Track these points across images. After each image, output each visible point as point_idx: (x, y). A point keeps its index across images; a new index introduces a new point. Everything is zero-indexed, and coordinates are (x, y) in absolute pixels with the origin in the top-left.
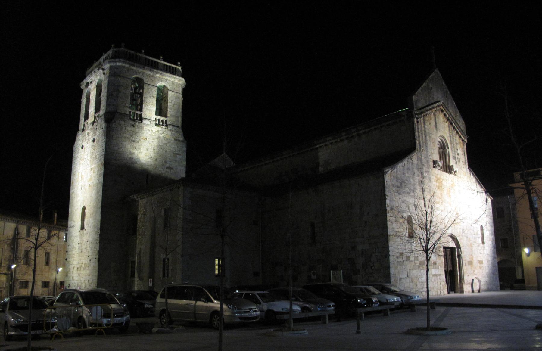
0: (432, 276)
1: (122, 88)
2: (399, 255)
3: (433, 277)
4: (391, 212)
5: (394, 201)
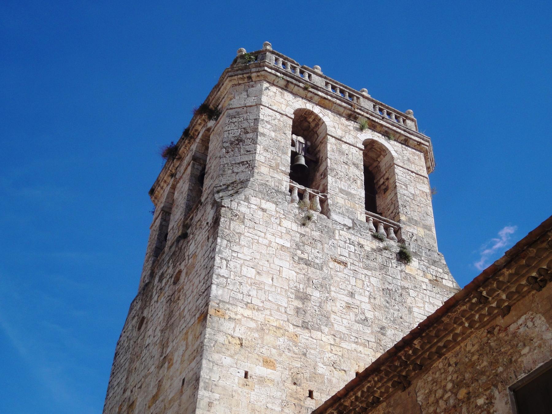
1: (269, 126)
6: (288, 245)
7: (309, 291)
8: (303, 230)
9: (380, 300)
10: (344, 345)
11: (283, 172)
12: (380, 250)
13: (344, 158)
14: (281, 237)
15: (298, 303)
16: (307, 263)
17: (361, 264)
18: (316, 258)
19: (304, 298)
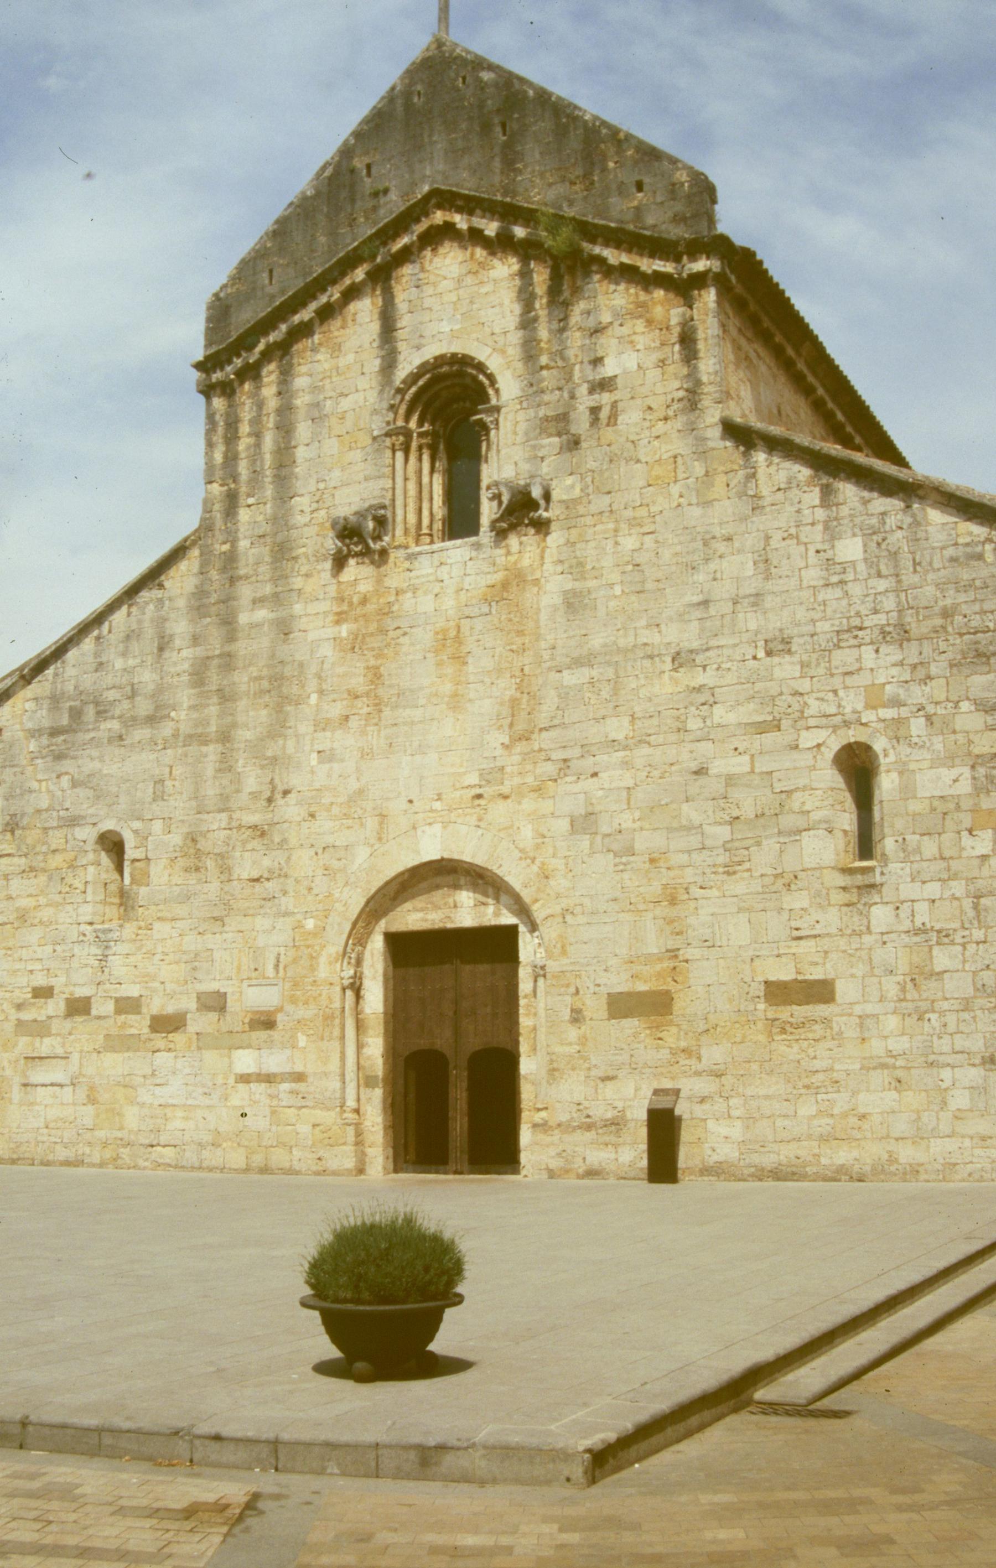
0: (231, 1081)
2: (30, 995)
4: (8, 835)
5: (30, 791)
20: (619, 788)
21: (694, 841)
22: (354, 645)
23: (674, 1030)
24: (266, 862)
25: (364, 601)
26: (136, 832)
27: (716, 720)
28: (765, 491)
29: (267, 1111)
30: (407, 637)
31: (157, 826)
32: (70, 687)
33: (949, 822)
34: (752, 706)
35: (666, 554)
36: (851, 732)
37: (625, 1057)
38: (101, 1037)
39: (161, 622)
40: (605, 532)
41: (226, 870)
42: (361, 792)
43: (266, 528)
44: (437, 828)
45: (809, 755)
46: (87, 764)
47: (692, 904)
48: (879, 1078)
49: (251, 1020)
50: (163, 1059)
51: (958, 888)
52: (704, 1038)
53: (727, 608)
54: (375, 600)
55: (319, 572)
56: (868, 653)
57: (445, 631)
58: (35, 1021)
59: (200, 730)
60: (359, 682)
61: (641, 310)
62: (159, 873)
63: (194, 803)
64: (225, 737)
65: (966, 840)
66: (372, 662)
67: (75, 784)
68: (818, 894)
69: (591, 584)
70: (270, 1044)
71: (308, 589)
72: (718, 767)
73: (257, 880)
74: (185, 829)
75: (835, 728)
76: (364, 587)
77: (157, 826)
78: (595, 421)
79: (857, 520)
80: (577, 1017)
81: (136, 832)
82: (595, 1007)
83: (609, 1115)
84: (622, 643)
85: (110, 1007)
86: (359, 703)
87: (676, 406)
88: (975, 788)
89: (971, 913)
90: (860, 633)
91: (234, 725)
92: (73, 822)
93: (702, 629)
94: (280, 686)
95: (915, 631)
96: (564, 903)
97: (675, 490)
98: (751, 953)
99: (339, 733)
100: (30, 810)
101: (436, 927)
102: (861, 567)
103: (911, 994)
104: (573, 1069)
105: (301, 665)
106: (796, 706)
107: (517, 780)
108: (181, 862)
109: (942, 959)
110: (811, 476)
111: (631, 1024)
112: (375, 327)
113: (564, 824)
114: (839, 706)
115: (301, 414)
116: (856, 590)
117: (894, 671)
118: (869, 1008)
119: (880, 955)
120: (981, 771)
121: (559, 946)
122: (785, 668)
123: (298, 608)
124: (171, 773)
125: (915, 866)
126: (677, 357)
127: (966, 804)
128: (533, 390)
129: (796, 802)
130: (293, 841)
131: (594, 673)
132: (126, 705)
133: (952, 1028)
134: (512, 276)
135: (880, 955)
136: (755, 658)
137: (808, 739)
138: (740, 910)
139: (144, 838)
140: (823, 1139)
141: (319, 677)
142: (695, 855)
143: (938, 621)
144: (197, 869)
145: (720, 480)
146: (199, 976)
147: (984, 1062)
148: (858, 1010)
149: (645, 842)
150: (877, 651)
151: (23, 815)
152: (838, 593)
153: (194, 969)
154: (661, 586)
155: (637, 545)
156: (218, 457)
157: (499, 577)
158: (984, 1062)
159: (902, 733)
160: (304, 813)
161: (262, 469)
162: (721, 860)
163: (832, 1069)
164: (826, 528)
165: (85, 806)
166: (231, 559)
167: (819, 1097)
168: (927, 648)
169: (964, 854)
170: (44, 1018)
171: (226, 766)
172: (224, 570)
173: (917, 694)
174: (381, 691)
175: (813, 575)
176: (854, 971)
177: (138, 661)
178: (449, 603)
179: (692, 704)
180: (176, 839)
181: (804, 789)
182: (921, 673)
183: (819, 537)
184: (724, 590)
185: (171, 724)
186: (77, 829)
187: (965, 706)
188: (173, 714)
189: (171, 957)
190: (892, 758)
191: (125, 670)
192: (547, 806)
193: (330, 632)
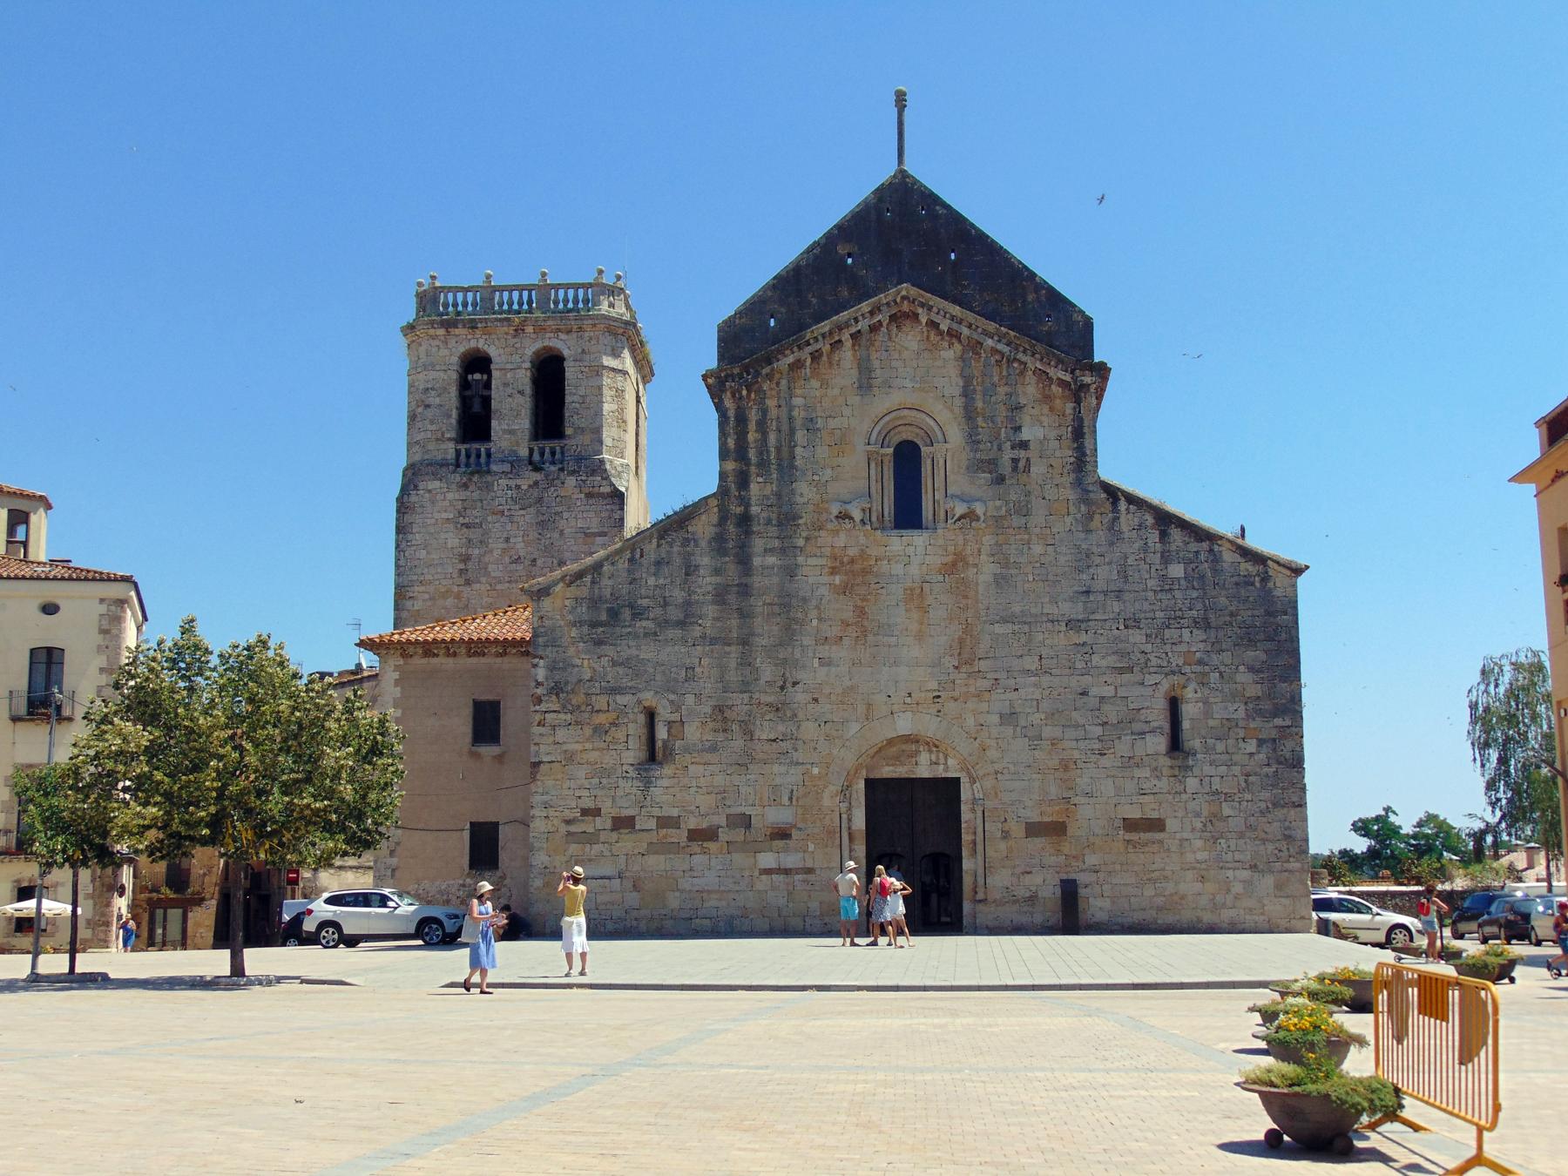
0: (756, 873)
1: (433, 393)
3: (764, 877)
6: (451, 516)
7: (470, 552)
8: (464, 494)
9: (533, 535)
10: (499, 587)
11: (450, 439)
12: (536, 483)
13: (509, 391)
14: (445, 511)
15: (462, 566)
16: (467, 526)
17: (517, 507)
18: (476, 517)
19: (466, 559)
20: (1032, 700)
21: (1081, 733)
22: (845, 590)
23: (1066, 844)
24: (781, 728)
25: (852, 561)
26: (672, 702)
27: (1094, 663)
28: (1125, 528)
29: (786, 895)
30: (884, 591)
31: (690, 699)
32: (607, 593)
33: (1231, 733)
34: (1114, 657)
35: (1062, 559)
36: (1175, 678)
37: (1036, 861)
38: (645, 846)
39: (687, 557)
40: (1021, 540)
41: (749, 735)
42: (852, 688)
43: (773, 500)
44: (909, 714)
45: (1151, 689)
46: (628, 650)
47: (1079, 771)
48: (1190, 875)
49: (771, 834)
50: (697, 859)
51: (1236, 770)
52: (1087, 851)
53: (1101, 597)
54: (860, 562)
55: (816, 537)
56: (1186, 632)
57: (912, 590)
58: (585, 832)
59: (723, 636)
60: (849, 615)
61: (1047, 398)
62: (693, 732)
63: (720, 685)
64: (745, 642)
65: (1242, 745)
66: (859, 603)
67: (614, 664)
68: (1156, 769)
69: (1013, 571)
70: (786, 850)
71: (809, 549)
72: (1094, 691)
73: (774, 740)
74: (713, 702)
75: (1166, 674)
76: (852, 552)
77: (690, 699)
78: (1015, 469)
79: (1181, 555)
80: (1006, 835)
81: (672, 702)
82: (1018, 830)
83: (1027, 895)
84: (1033, 611)
85: (652, 824)
86: (850, 628)
87: (1069, 467)
88: (1247, 715)
89: (1243, 785)
90: (1182, 621)
91: (753, 635)
92: (615, 691)
93: (1085, 609)
94: (789, 611)
95: (1213, 624)
96: (996, 766)
97: (1068, 520)
98: (1114, 801)
99: (834, 648)
100: (574, 680)
101: (903, 776)
102: (1183, 582)
103: (1209, 827)
104: (1003, 867)
105: (805, 600)
106: (1142, 661)
107: (964, 689)
108: (711, 725)
109: (1227, 810)
110: (1154, 524)
111: (1039, 842)
112: (855, 372)
113: (995, 719)
114: (1169, 662)
115: (798, 423)
116: (1178, 594)
117: (1202, 646)
118: (1185, 835)
119: (1192, 805)
120: (1251, 706)
121: (993, 792)
122: (1136, 637)
123: (800, 560)
124: (700, 662)
125: (1212, 757)
126: (1069, 435)
127: (1240, 724)
128: (973, 440)
129: (1143, 715)
130: (801, 715)
131: (1016, 628)
132: (658, 611)
133: (1233, 848)
134: (956, 359)
135: (1192, 805)
136: (1118, 629)
137: (1150, 679)
138: (1108, 776)
139: (676, 707)
140: (1160, 909)
141: (818, 607)
142: (1081, 743)
143: (1228, 618)
144: (725, 731)
145: (1097, 517)
146: (728, 803)
147: (1251, 867)
148: (1178, 836)
149: (1048, 732)
150: (1191, 632)
151: (567, 683)
152: (1169, 596)
153: (724, 798)
154: (1058, 578)
155: (1043, 552)
156: (731, 442)
157: (950, 559)
158: (1251, 867)
159: (1204, 681)
160: (809, 697)
161: (768, 456)
162: (1097, 746)
163: (1163, 870)
164: (1162, 557)
165: (624, 680)
166: (745, 520)
167: (1157, 885)
168: (1221, 634)
169: (1241, 752)
170: (592, 830)
171: (746, 662)
172: (738, 525)
173: (1215, 659)
174: (866, 623)
175: (1152, 583)
176: (1176, 814)
177: (669, 580)
178: (914, 570)
179: (1078, 652)
180: (708, 710)
181: (1147, 708)
182: (1217, 646)
183: (1158, 562)
184: (1099, 585)
185: (699, 628)
186: (618, 697)
187: (1242, 668)
188: (700, 622)
189: (705, 790)
190: (1199, 695)
191: (657, 586)
192: (984, 707)
193: (826, 579)
